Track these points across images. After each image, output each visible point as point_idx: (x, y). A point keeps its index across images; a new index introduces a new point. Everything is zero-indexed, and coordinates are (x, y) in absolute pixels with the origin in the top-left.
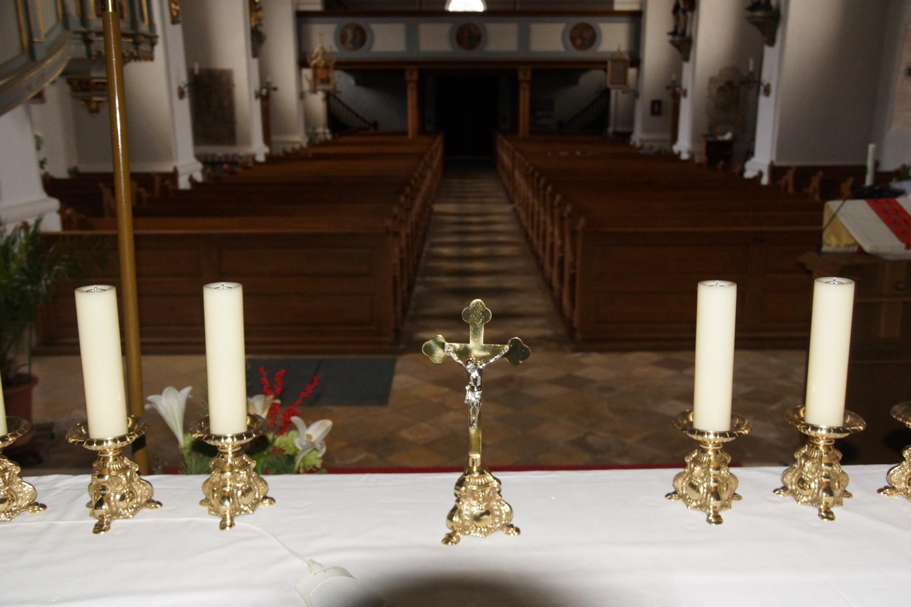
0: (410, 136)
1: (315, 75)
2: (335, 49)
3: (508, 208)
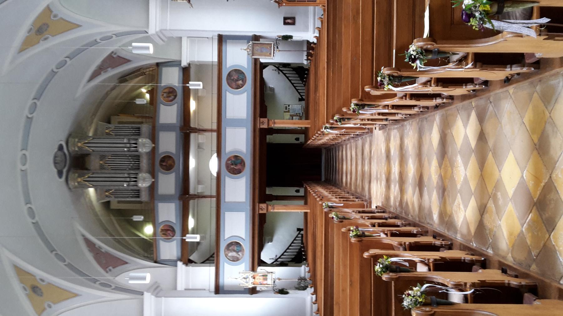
0: (309, 211)
3: (378, 134)
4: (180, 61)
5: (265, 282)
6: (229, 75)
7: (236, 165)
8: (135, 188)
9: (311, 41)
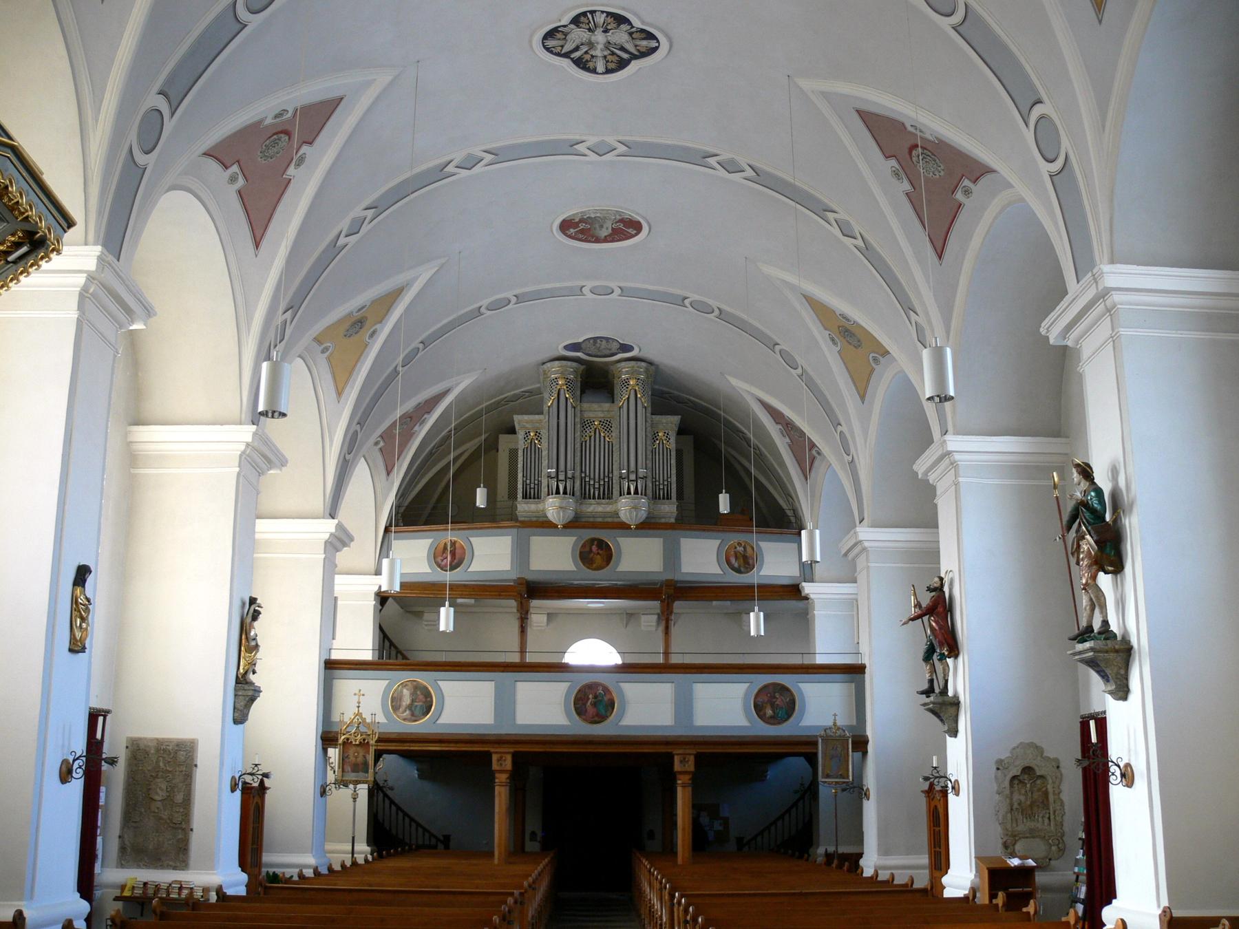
0: (496, 861)
1: (343, 759)
2: (381, 718)
4: (812, 580)
5: (348, 768)
6: (784, 689)
7: (594, 705)
8: (544, 490)
9: (862, 862)
